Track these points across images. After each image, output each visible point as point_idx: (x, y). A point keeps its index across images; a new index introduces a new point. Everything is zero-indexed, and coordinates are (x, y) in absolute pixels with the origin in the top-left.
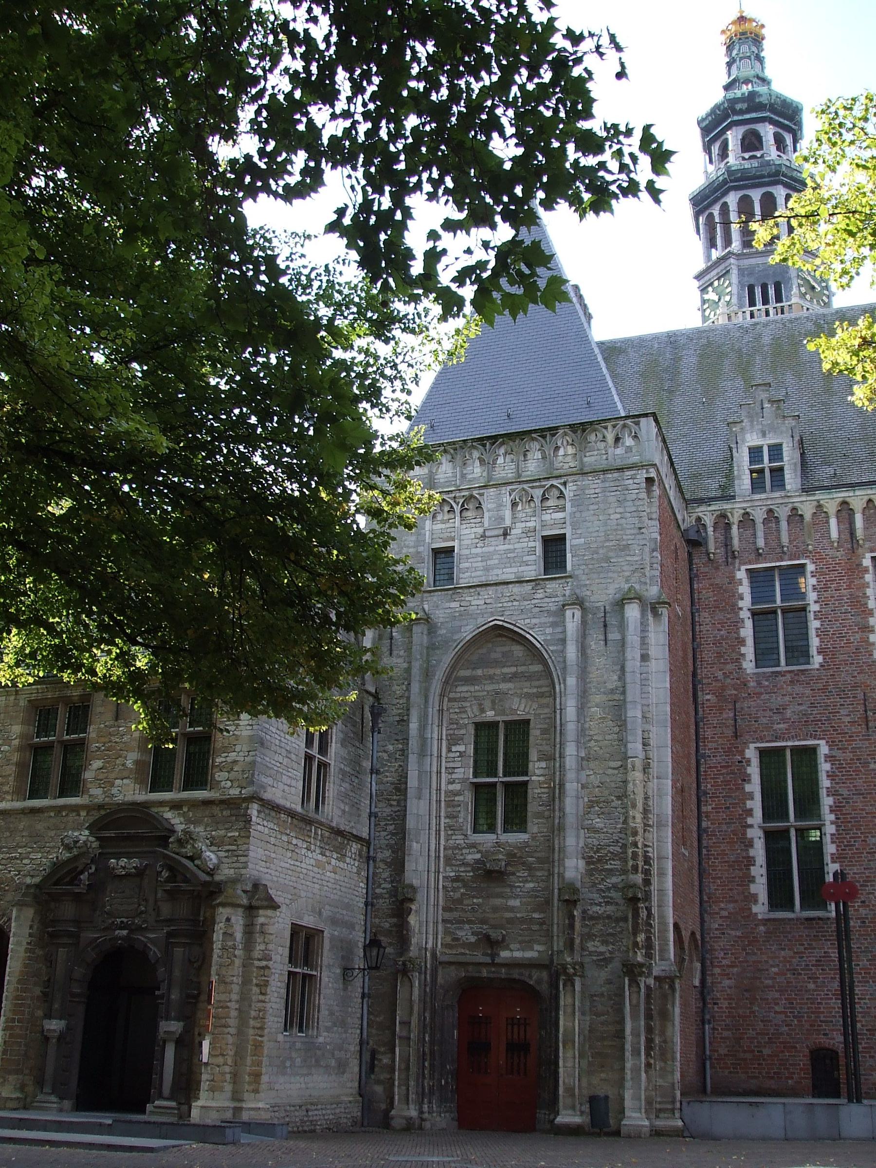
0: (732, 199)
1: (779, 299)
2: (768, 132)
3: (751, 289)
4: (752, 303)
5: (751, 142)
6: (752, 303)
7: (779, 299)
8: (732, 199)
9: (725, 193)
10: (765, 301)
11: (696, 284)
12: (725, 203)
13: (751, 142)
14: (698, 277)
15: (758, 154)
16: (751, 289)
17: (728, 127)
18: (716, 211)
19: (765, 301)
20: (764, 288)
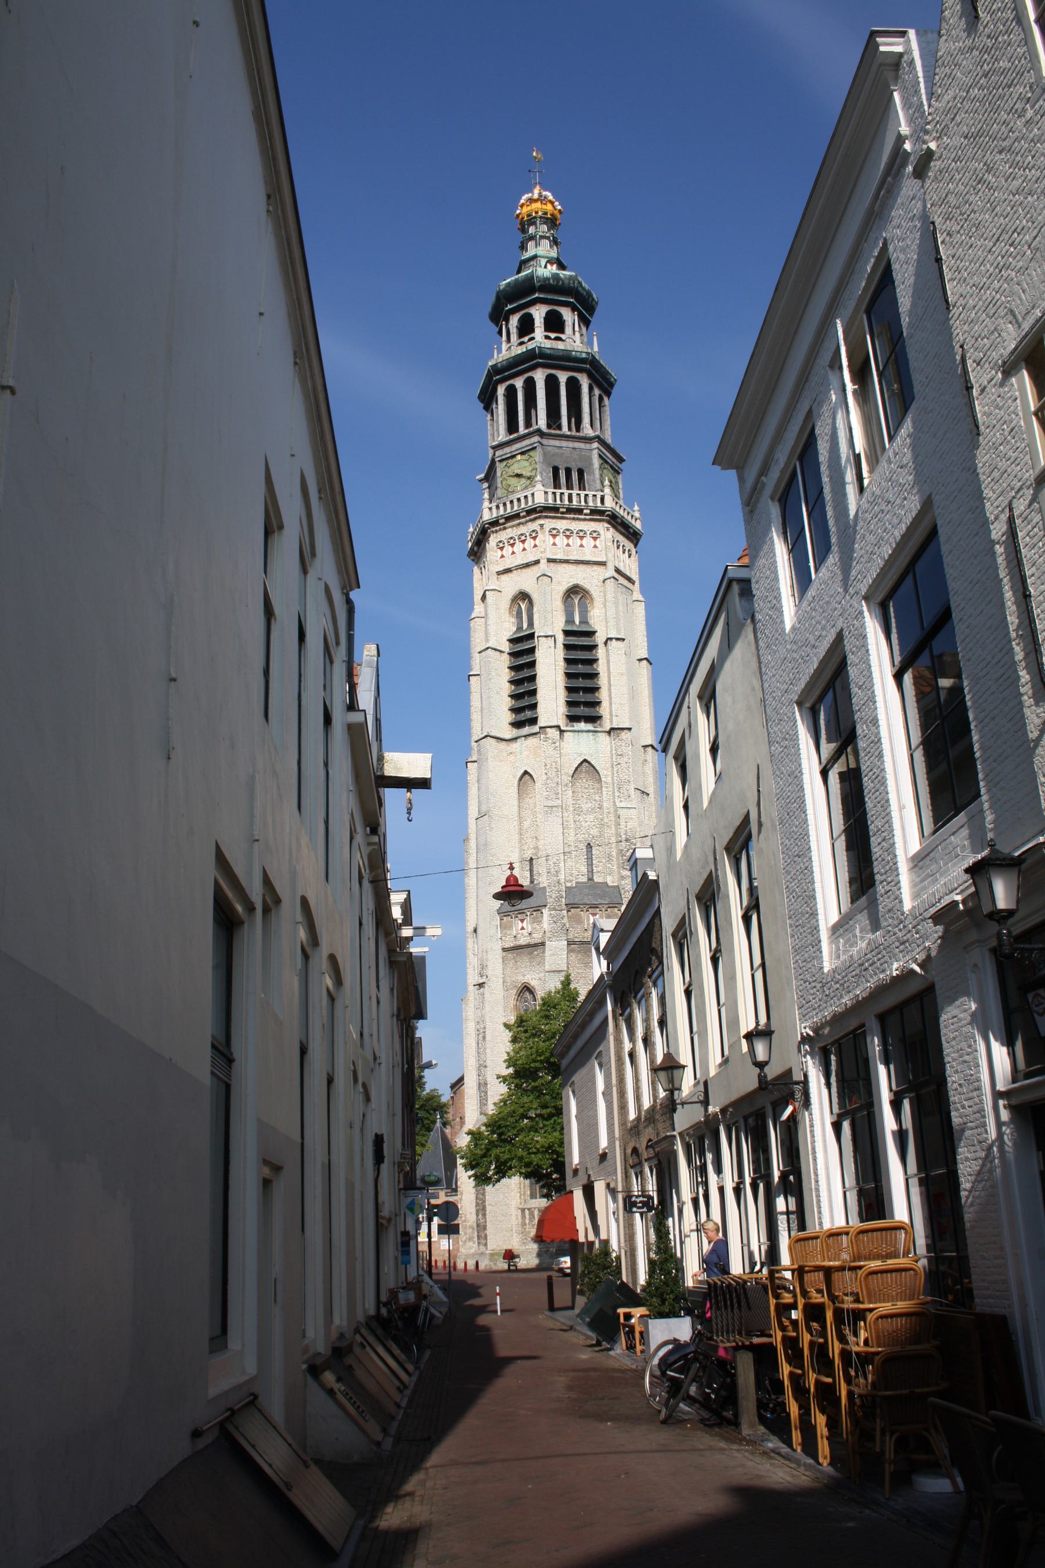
8: (540, 377)
16: (556, 471)
18: (519, 383)
20: (568, 471)
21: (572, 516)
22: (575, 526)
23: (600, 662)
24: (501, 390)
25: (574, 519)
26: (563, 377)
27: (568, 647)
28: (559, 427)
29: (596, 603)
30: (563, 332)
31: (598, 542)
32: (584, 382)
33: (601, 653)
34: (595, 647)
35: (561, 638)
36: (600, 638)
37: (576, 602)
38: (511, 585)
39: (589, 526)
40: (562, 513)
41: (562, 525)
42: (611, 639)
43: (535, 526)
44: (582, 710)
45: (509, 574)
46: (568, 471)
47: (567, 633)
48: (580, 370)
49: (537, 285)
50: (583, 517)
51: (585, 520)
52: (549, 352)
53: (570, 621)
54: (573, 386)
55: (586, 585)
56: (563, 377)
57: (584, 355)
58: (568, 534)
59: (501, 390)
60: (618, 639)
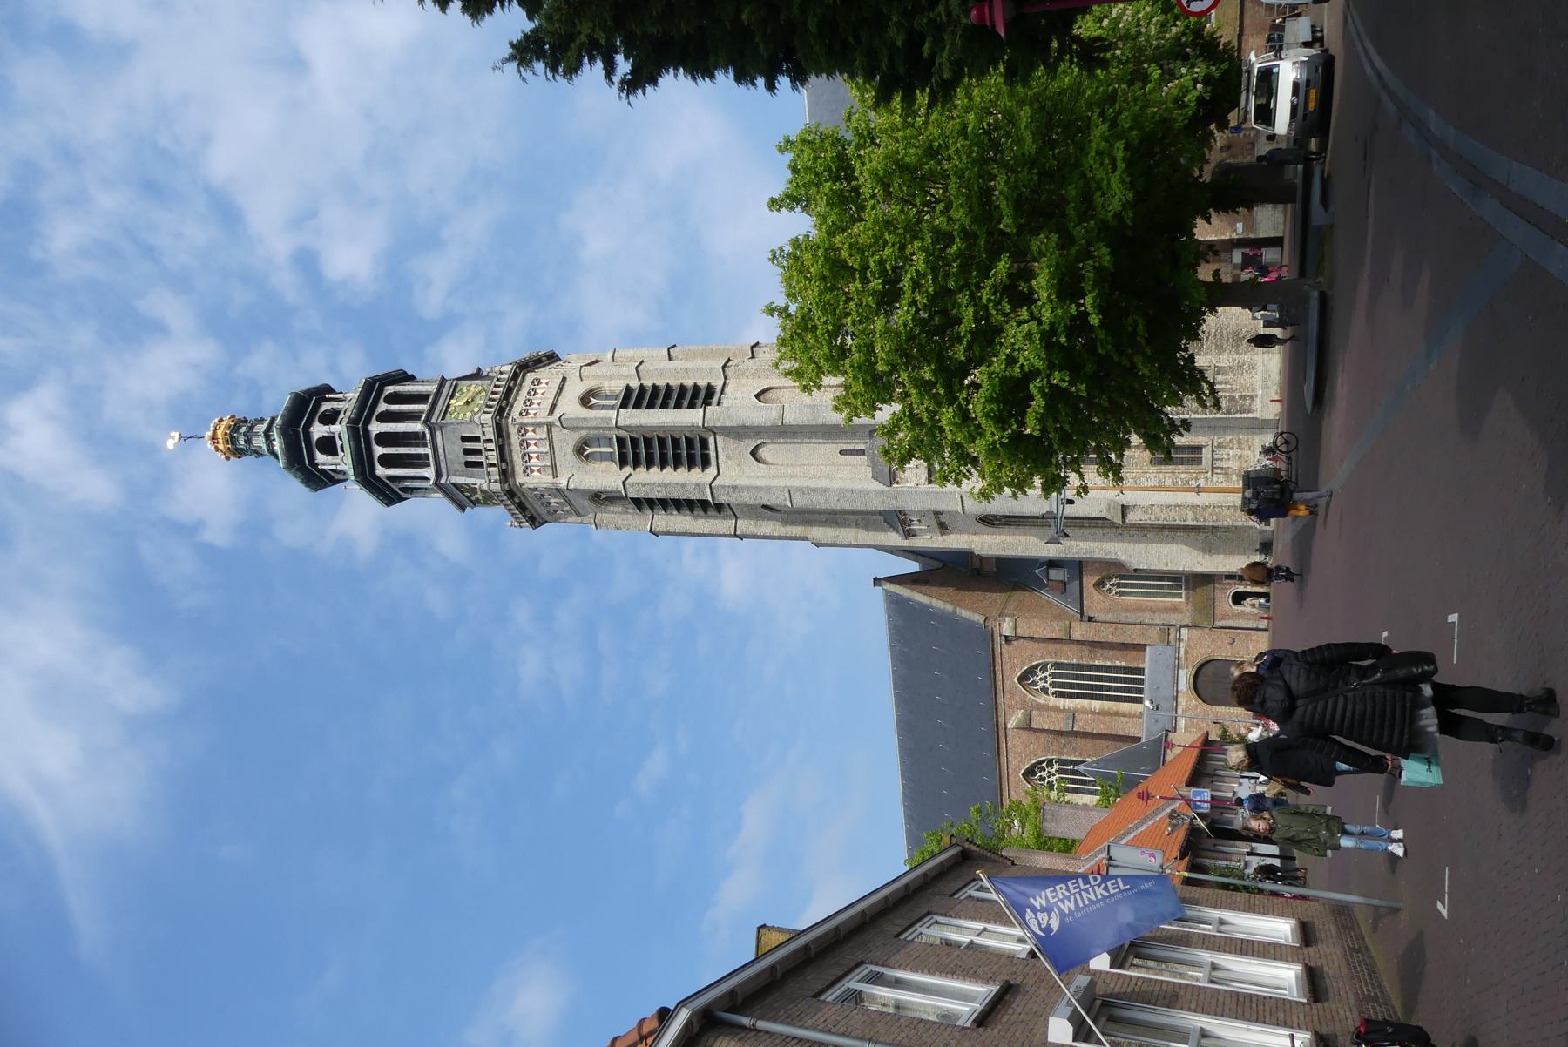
0: (381, 471)
1: (476, 439)
2: (318, 431)
3: (469, 464)
4: (480, 464)
5: (328, 445)
6: (480, 464)
7: (476, 439)
8: (381, 471)
9: (378, 478)
10: (478, 452)
11: (468, 509)
13: (328, 445)
14: (463, 509)
15: (339, 443)
16: (469, 464)
17: (315, 465)
19: (478, 452)
20: (467, 452)
26: (379, 451)
27: (636, 464)
30: (333, 438)
32: (376, 428)
35: (628, 469)
44: (698, 452)
46: (467, 452)
48: (367, 433)
53: (610, 457)
54: (384, 439)
56: (379, 451)
58: (527, 457)
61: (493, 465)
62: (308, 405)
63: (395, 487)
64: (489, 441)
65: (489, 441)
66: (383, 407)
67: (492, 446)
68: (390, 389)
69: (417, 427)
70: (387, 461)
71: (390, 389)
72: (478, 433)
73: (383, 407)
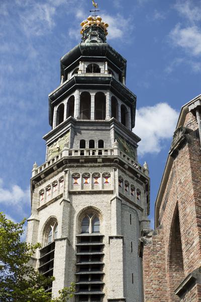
8: (77, 94)
9: (73, 91)
12: (73, 97)
18: (65, 102)
21: (89, 164)
22: (91, 171)
23: (105, 257)
24: (56, 109)
25: (91, 167)
26: (93, 95)
28: (89, 118)
29: (104, 217)
31: (109, 180)
33: (105, 251)
34: (103, 246)
35: (75, 243)
36: (105, 241)
37: (91, 220)
38: (44, 217)
39: (101, 171)
40: (82, 163)
41: (81, 171)
42: (111, 238)
43: (63, 174)
45: (47, 208)
47: (81, 239)
48: (106, 88)
49: (82, 51)
50: (97, 164)
51: (99, 166)
52: (83, 79)
54: (100, 100)
55: (98, 207)
56: (93, 95)
57: (107, 79)
59: (56, 109)
60: (117, 237)
61: (82, 153)
62: (118, 64)
63: (65, 102)
64: (100, 153)
65: (100, 153)
66: (120, 103)
67: (97, 154)
68: (129, 110)
69: (108, 118)
70: (85, 100)
71: (129, 110)
72: (105, 148)
73: (120, 103)
